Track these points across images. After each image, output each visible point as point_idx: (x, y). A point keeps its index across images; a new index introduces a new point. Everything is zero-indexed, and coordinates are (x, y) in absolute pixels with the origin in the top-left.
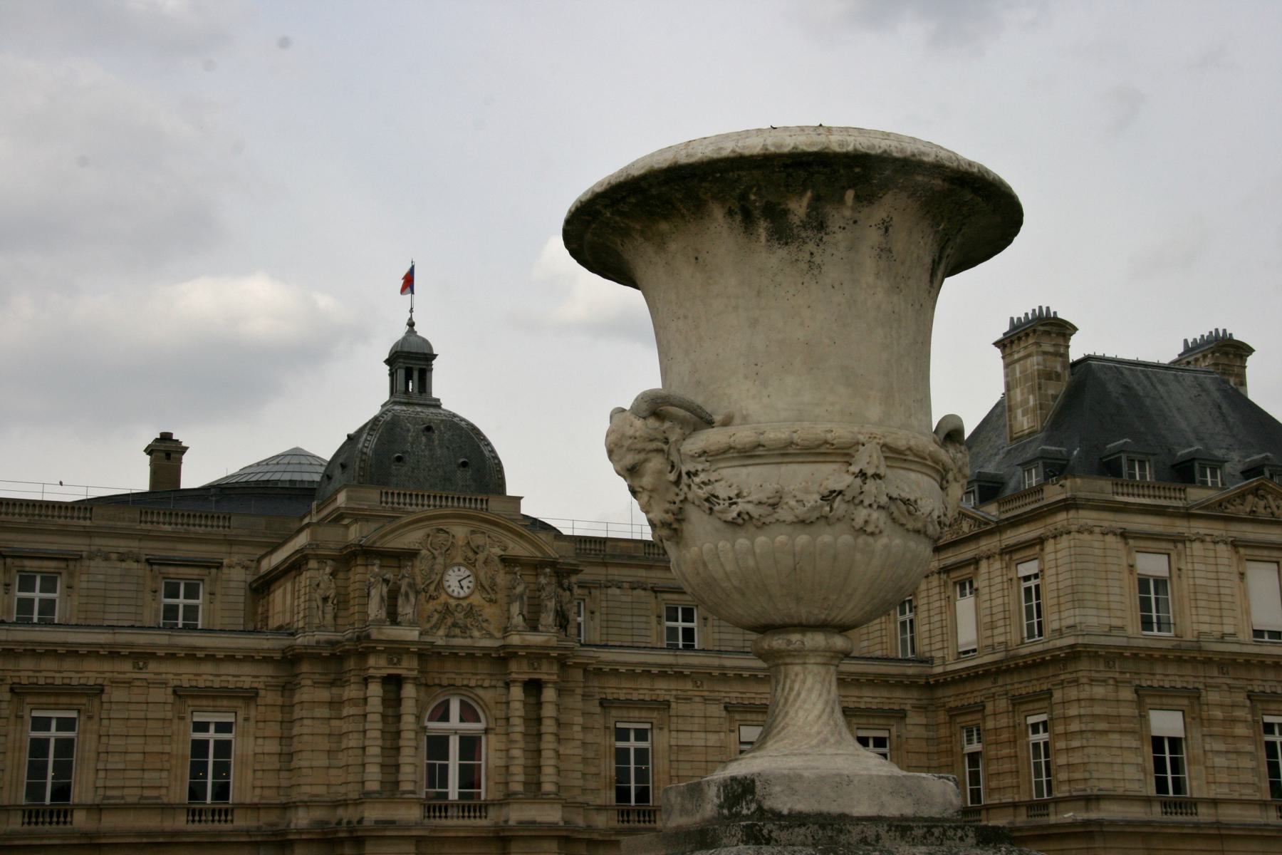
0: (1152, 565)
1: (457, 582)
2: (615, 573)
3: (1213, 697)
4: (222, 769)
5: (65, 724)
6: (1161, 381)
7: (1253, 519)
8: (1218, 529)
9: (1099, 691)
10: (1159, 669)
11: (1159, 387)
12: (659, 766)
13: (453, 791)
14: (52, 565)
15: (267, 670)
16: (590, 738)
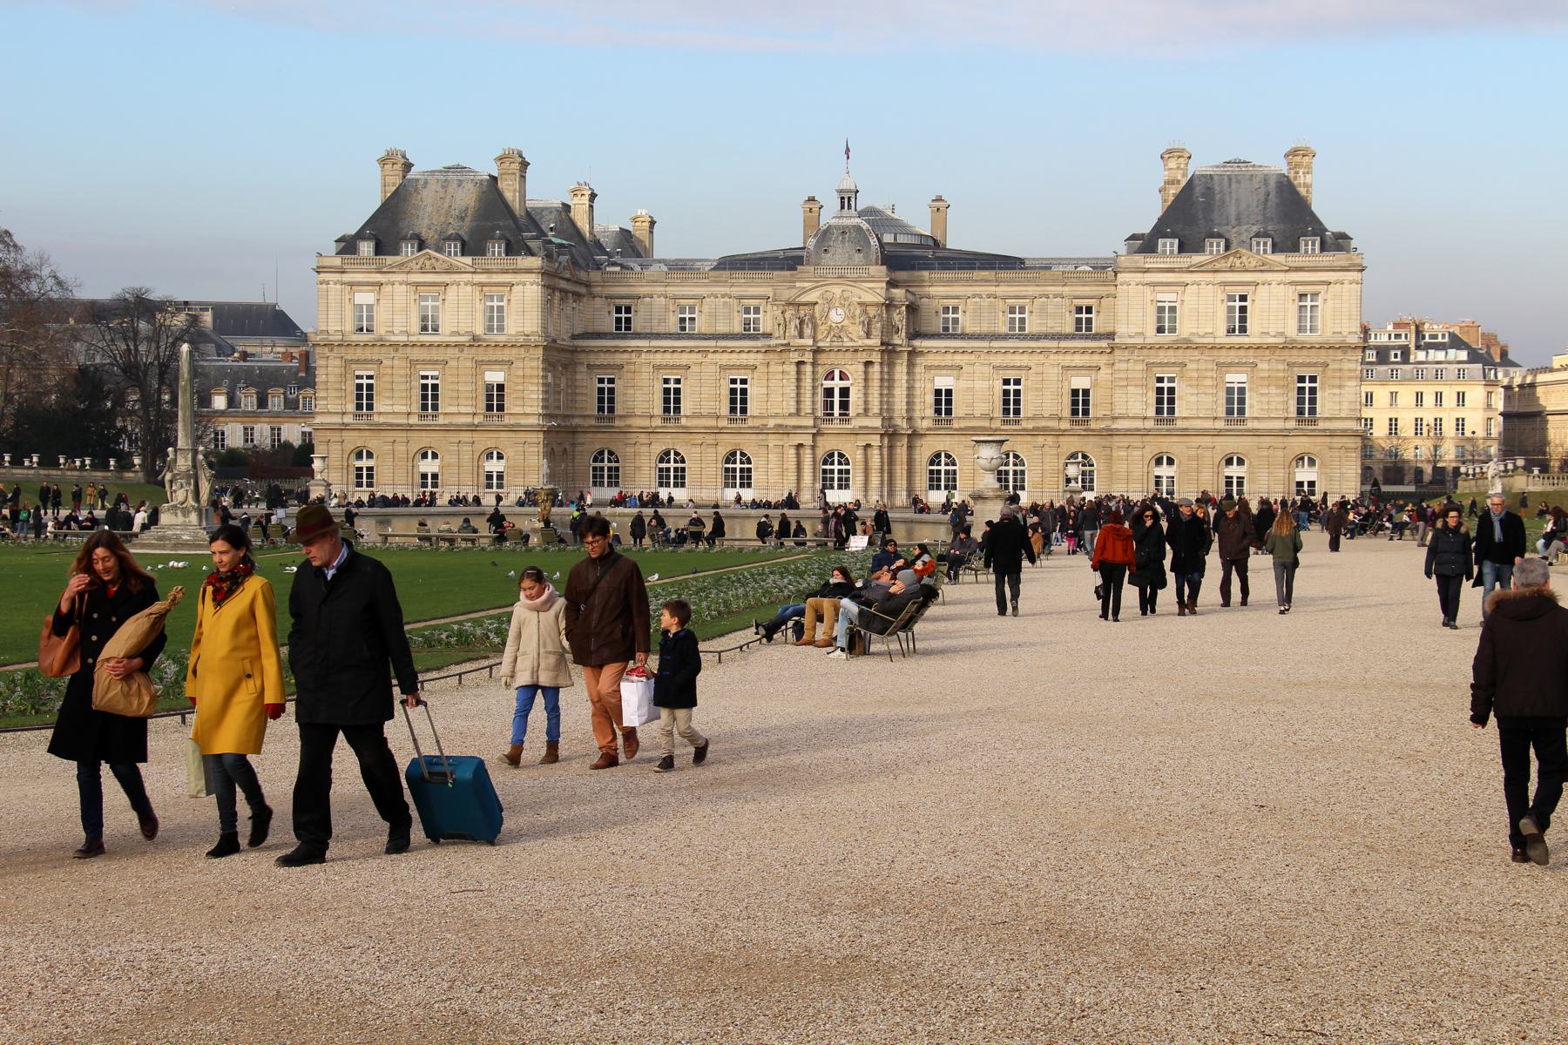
0: (1167, 297)
1: (836, 316)
2: (978, 290)
3: (1194, 366)
4: (744, 401)
5: (678, 381)
6: (1238, 182)
7: (1232, 270)
8: (1209, 277)
10: (1162, 353)
11: (1234, 186)
13: (837, 411)
14: (691, 302)
15: (760, 356)
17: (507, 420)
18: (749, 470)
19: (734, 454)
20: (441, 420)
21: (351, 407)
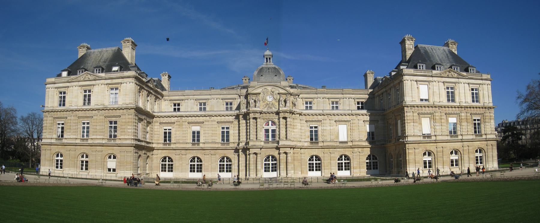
3: (436, 114)
9: (408, 114)
12: (320, 133)
13: (270, 139)
16: (303, 128)
17: (118, 142)
18: (230, 165)
19: (223, 158)
20: (90, 141)
21: (55, 136)
